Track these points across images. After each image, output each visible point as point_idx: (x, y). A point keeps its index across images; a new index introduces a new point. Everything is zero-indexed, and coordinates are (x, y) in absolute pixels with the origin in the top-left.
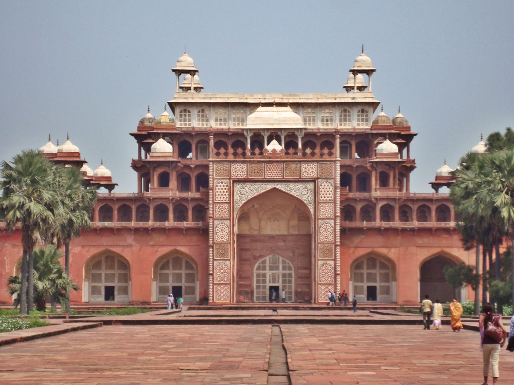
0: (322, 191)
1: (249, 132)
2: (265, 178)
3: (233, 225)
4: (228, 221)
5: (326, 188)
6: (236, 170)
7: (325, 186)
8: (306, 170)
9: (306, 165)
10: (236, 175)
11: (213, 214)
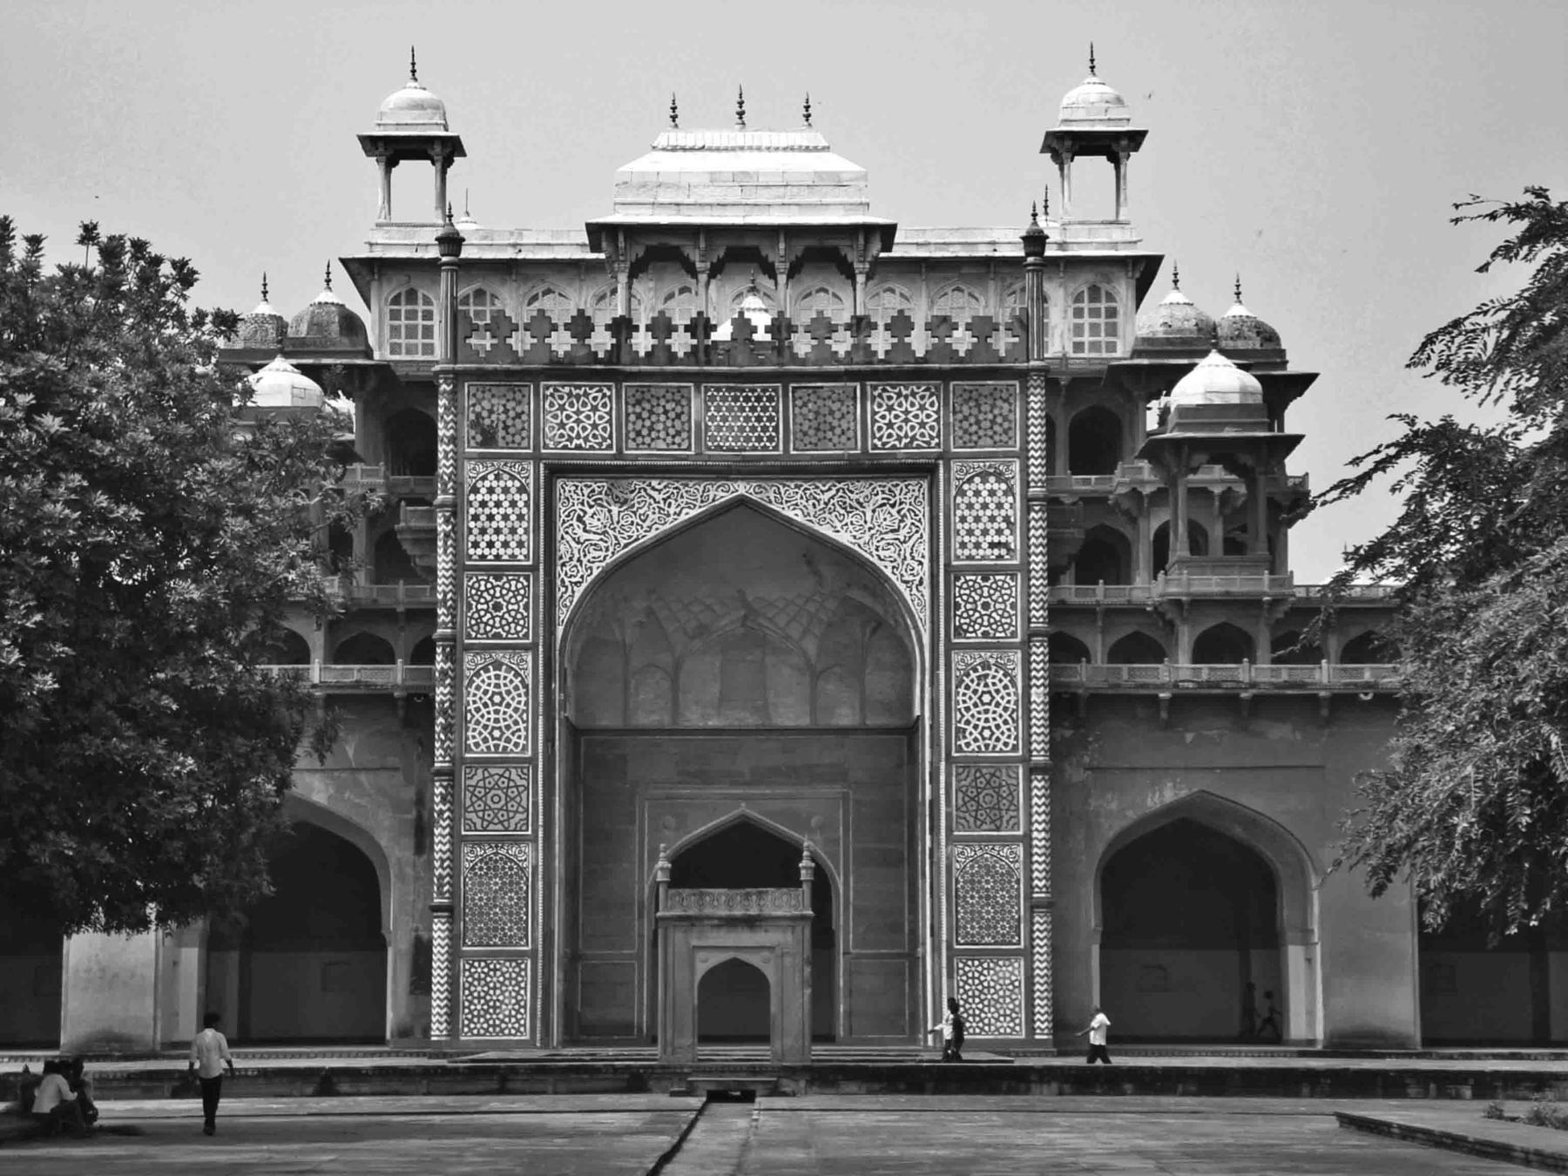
0: (963, 519)
5: (985, 506)
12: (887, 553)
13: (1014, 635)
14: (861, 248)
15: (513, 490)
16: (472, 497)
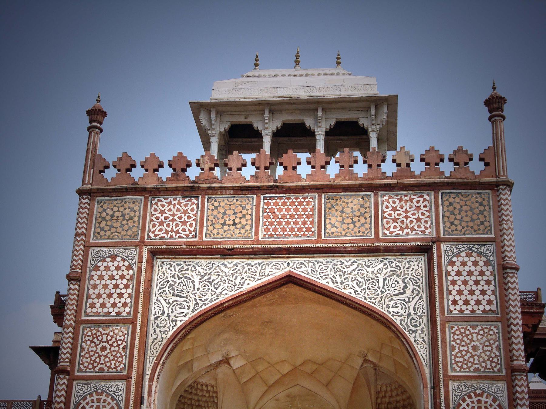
0: (454, 283)
1: (213, 116)
2: (257, 241)
3: (140, 400)
4: (122, 386)
5: (470, 273)
6: (162, 218)
7: (464, 264)
8: (394, 215)
9: (396, 199)
10: (161, 234)
11: (72, 361)
12: (396, 310)
13: (500, 370)
14: (373, 114)
15: (123, 268)
16: (93, 273)
